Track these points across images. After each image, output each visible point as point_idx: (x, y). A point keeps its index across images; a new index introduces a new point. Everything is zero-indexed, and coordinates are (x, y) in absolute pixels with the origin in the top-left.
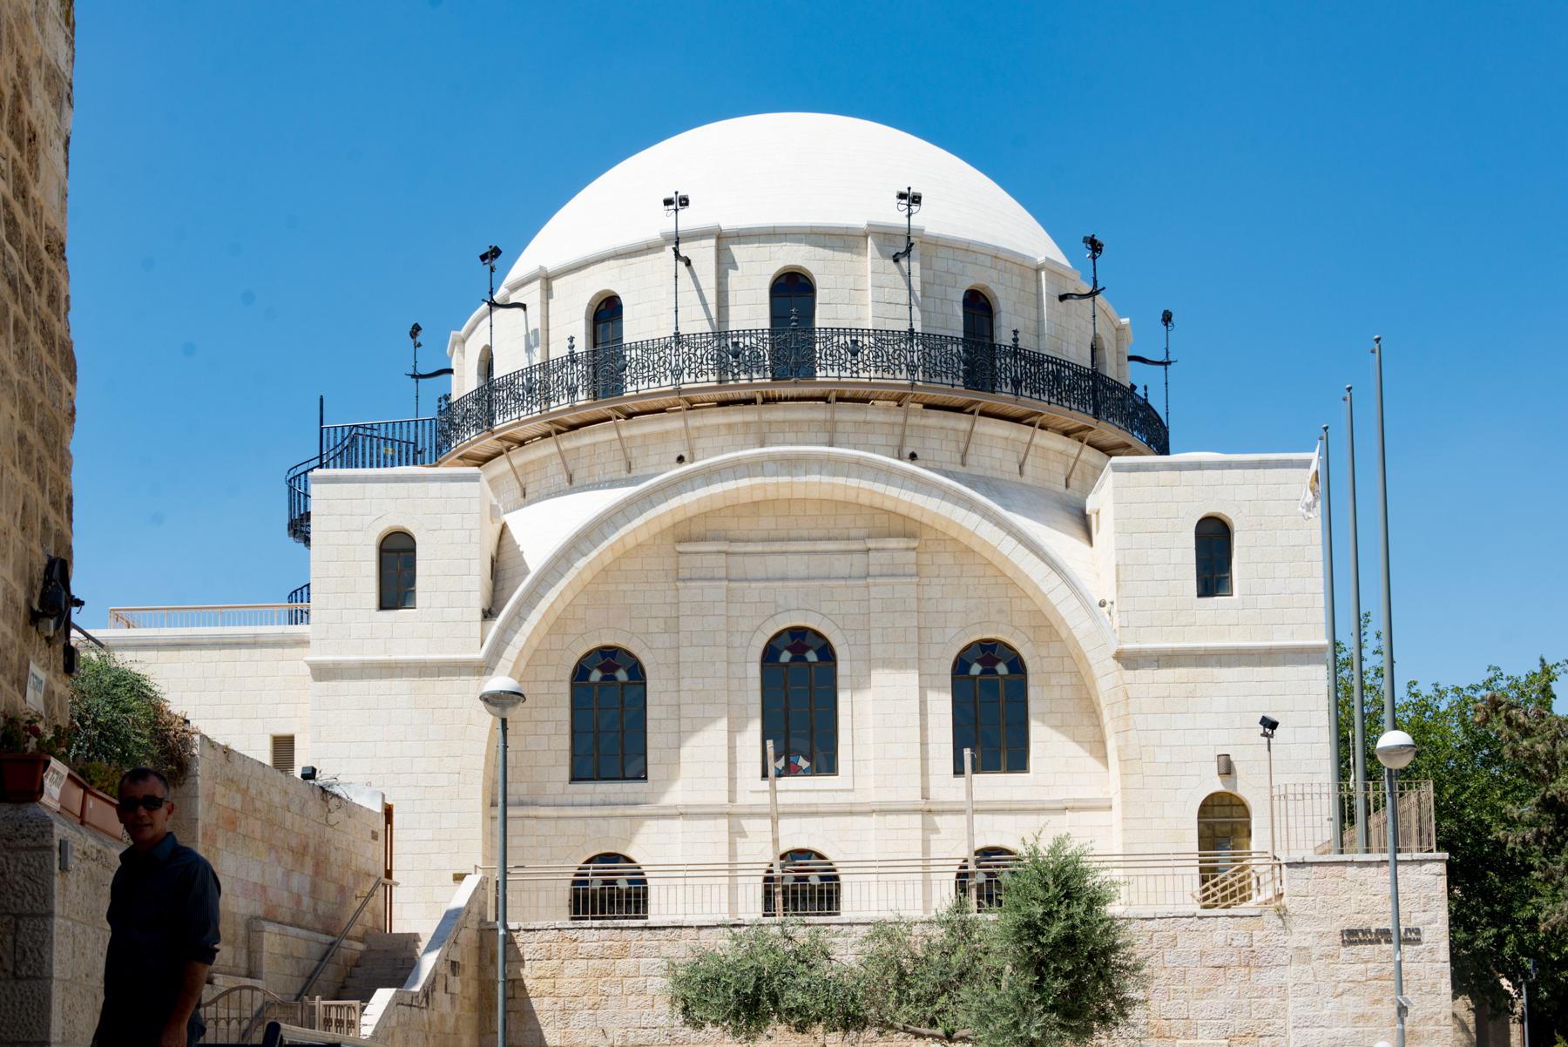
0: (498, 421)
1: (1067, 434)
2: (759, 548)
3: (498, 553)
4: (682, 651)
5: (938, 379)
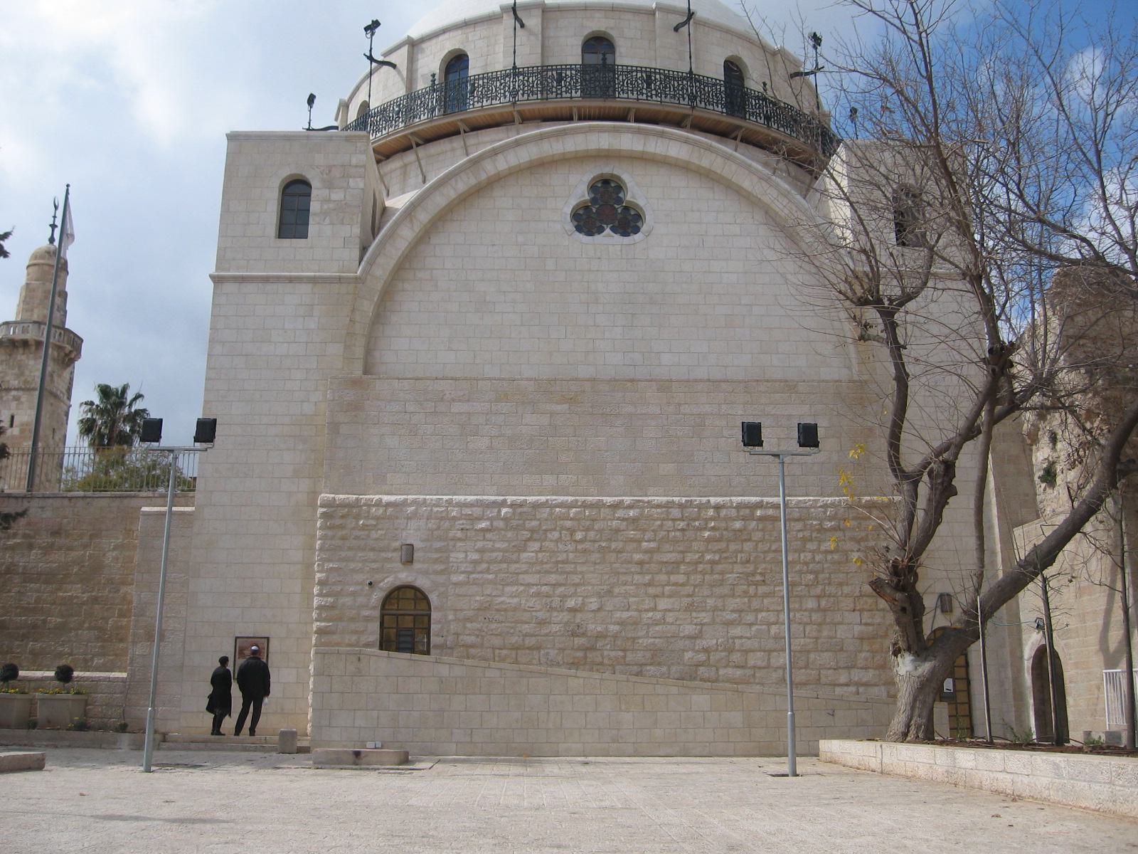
5: (711, 107)
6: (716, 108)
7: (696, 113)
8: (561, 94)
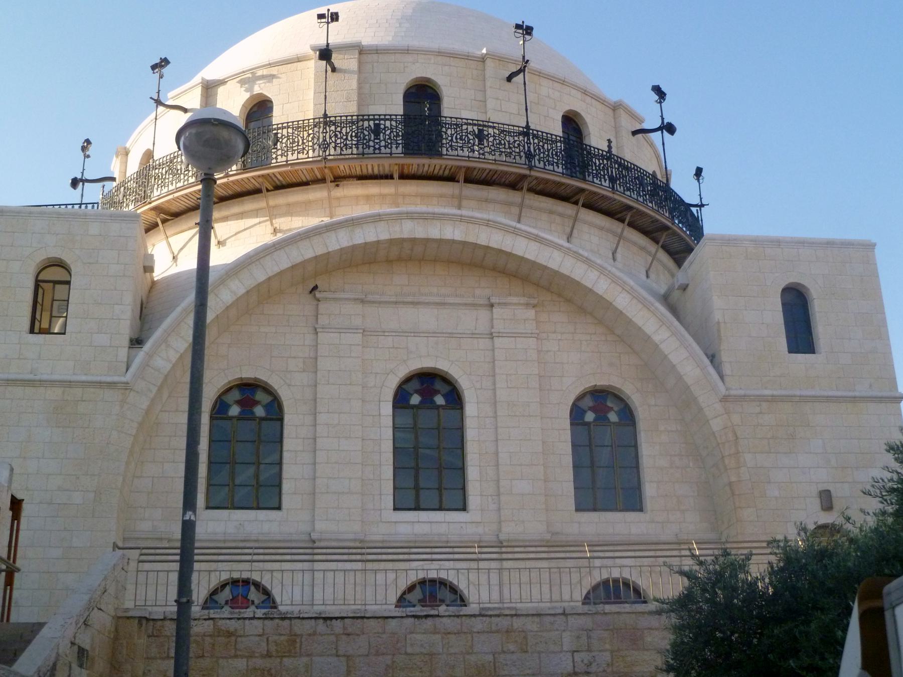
0: (156, 193)
1: (646, 232)
2: (393, 299)
3: (148, 297)
4: (319, 387)
5: (551, 168)
6: (556, 168)
7: (533, 173)
8: (379, 149)
